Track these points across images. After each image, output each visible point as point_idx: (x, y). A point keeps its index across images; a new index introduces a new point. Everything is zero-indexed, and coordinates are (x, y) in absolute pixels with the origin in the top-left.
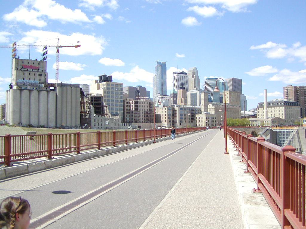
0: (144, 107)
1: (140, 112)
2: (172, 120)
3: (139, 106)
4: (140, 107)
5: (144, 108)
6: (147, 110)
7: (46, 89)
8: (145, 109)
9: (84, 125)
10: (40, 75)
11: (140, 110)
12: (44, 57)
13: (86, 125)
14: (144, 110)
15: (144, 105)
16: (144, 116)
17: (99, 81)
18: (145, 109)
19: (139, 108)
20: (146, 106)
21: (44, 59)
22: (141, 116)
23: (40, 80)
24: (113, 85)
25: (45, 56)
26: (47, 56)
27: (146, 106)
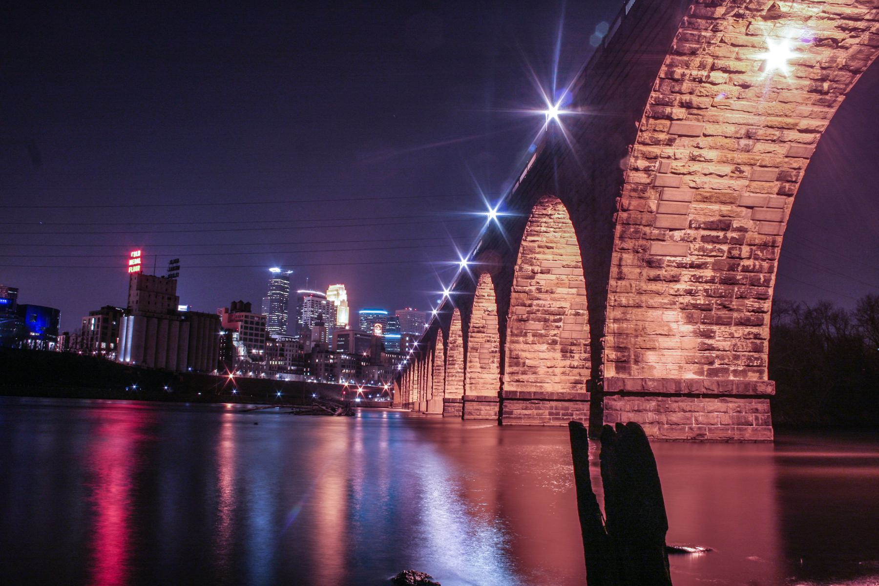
3: (285, 350)
5: (291, 353)
6: (296, 356)
7: (178, 318)
8: (293, 355)
10: (169, 299)
11: (286, 355)
12: (172, 272)
14: (291, 356)
17: (231, 310)
19: (285, 353)
21: (171, 276)
23: (169, 305)
24: (253, 317)
25: (175, 272)
26: (178, 273)
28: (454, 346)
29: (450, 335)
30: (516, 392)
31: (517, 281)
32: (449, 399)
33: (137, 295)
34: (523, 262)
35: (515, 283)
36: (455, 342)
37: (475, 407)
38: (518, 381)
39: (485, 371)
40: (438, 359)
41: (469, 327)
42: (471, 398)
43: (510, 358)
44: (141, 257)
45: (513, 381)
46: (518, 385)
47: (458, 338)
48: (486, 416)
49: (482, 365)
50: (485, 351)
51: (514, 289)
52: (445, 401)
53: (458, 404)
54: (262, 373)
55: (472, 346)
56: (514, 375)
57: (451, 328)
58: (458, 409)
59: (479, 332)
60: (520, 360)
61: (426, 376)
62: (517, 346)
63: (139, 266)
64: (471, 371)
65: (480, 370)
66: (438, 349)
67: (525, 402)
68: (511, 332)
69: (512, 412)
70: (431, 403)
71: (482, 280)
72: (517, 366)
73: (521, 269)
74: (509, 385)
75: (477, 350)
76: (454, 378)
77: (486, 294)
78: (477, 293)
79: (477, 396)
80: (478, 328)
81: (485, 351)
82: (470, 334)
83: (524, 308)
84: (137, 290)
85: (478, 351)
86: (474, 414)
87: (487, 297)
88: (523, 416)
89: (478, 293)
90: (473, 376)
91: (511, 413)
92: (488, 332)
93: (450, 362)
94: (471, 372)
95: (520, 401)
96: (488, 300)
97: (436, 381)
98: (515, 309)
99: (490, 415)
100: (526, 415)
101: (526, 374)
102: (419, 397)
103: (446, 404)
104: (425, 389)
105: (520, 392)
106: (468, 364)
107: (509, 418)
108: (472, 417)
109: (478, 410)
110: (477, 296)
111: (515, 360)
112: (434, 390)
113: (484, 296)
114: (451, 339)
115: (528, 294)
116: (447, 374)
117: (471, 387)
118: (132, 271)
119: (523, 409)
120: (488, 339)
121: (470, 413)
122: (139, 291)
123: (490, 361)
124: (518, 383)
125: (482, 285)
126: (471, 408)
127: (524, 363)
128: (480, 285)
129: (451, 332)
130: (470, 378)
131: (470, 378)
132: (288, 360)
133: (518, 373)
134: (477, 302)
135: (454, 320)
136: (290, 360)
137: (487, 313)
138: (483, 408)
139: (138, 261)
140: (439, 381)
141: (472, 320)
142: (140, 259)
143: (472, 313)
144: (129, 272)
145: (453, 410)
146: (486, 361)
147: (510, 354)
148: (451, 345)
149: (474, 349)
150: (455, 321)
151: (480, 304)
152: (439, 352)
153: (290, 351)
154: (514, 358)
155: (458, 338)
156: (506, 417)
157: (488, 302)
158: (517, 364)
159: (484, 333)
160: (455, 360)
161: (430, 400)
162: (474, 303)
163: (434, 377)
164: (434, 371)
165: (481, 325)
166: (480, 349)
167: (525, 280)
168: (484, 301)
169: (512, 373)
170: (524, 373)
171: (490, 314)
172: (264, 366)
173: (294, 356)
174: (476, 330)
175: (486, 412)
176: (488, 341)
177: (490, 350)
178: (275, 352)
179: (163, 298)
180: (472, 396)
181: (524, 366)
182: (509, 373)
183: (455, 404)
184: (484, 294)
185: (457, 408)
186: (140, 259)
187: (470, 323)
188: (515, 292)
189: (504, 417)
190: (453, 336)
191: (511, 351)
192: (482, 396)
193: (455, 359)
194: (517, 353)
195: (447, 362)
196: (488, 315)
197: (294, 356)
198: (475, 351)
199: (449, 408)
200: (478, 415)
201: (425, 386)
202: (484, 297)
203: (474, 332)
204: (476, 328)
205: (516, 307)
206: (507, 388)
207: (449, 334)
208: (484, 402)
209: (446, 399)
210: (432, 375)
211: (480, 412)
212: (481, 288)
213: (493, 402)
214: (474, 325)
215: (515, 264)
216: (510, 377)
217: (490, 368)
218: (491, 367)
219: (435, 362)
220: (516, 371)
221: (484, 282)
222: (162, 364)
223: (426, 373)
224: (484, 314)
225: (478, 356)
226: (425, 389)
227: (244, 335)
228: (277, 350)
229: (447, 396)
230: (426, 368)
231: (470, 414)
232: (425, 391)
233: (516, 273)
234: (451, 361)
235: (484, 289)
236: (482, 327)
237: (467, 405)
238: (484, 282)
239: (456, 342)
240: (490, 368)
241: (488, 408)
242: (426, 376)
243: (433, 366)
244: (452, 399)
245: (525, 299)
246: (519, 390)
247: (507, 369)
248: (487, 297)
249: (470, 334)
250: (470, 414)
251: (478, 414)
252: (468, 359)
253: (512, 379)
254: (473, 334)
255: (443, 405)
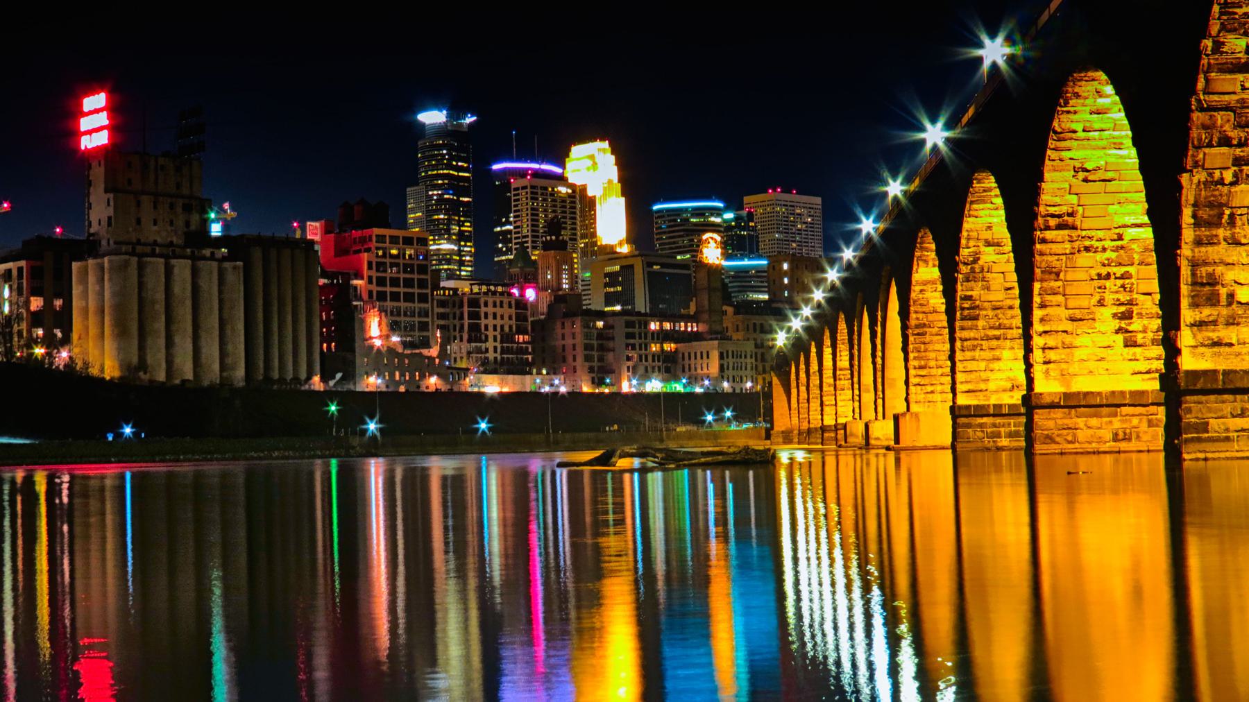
0: (498, 317)
1: (487, 337)
2: (596, 364)
4: (486, 317)
6: (510, 327)
8: (502, 327)
9: (334, 378)
13: (339, 376)
14: (499, 329)
15: (498, 310)
16: (499, 350)
18: (502, 327)
19: (483, 322)
20: (506, 317)
22: (491, 350)
23: (188, 224)
27: (506, 317)
28: (973, 270)
29: (963, 242)
30: (1215, 372)
31: (1207, 80)
32: (968, 407)
33: (109, 205)
34: (1223, 28)
35: (1201, 85)
36: (976, 260)
37: (1059, 422)
38: (1217, 344)
39: (1082, 327)
40: (919, 309)
41: (1035, 216)
42: (1047, 400)
43: (1194, 284)
44: (111, 108)
45: (1203, 345)
46: (1215, 354)
47: (983, 249)
48: (1090, 443)
49: (1071, 311)
50: (1081, 275)
51: (1199, 101)
52: (956, 412)
53: (991, 418)
54: (431, 375)
55: (1044, 265)
56: (1204, 328)
57: (966, 226)
58: (992, 432)
59: (1060, 227)
60: (1219, 287)
61: (879, 354)
62: (1212, 252)
63: (105, 133)
64: (1047, 328)
65: (1069, 326)
66: (918, 283)
67: (1239, 397)
68: (1194, 216)
69: (1207, 423)
70: (905, 424)
71: (1070, 89)
72: (1213, 305)
73: (1218, 45)
74: (1194, 355)
75: (1058, 274)
76: (977, 353)
77: (1078, 127)
78: (1056, 124)
79: (1065, 394)
80: (1059, 216)
81: (1081, 275)
82: (1038, 233)
83: (1224, 149)
84: (106, 191)
85: (1062, 276)
86: (1058, 439)
87: (1081, 134)
88: (1236, 434)
89: (1059, 125)
90: (1051, 343)
91: (1205, 427)
92: (1085, 226)
93: (966, 312)
94: (1046, 332)
95: (1226, 396)
96: (1085, 142)
97: (916, 363)
98: (1201, 156)
99: (1100, 440)
100: (1243, 430)
101: (1238, 324)
102: (857, 410)
103: (962, 420)
104: (880, 387)
105: (1226, 373)
106: (1037, 313)
107: (1199, 440)
108: (1054, 448)
109: (1070, 428)
110: (1056, 132)
111: (1208, 288)
112: (912, 389)
113: (1075, 132)
114: (964, 252)
115: (1234, 112)
116: (958, 344)
117: (1047, 372)
118: (89, 147)
119: (1234, 417)
120: (1087, 243)
121: (1048, 437)
122: (111, 196)
123: (1094, 300)
124: (1216, 349)
125: (1072, 102)
126: (1051, 424)
127: (1231, 296)
128: (1066, 104)
129: (964, 234)
130: (1044, 349)
131: (1044, 349)
132: (491, 339)
133: (1215, 323)
134: (1056, 149)
135: (972, 202)
136: (495, 340)
137: (1081, 175)
138: (1081, 422)
139: (102, 119)
140: (923, 363)
141: (1045, 198)
142: (105, 113)
143: (1042, 179)
144: (83, 148)
145: (980, 434)
146: (1084, 302)
147: (1194, 274)
148: (964, 269)
149: (1051, 273)
150: (975, 206)
151: (1066, 154)
152: (921, 291)
153: (495, 317)
154: (1203, 285)
155: (983, 249)
156: (1192, 440)
157: (1084, 148)
158: (1213, 300)
159: (1074, 228)
160: (978, 306)
161: (904, 414)
162: (1049, 152)
163: (911, 356)
164: (911, 339)
165: (1064, 209)
166: (1066, 271)
167: (1229, 76)
168: (1075, 143)
169: (1199, 325)
170: (1232, 322)
171: (1090, 178)
172: (434, 358)
173: (507, 329)
174: (1053, 222)
175: (1090, 432)
176: (1087, 249)
177: (1093, 273)
178: (457, 322)
179: (172, 206)
180: (1050, 394)
181: (1230, 304)
182: (1193, 325)
183: (985, 420)
184: (1074, 126)
185: (989, 430)
186: (105, 113)
187: (1038, 205)
188: (1202, 109)
189: (1187, 441)
190: (972, 243)
191: (1194, 265)
192: (1079, 393)
193: (977, 303)
194: (1210, 269)
195: (958, 314)
196: (1086, 180)
197: (507, 329)
198: (1053, 276)
199: (970, 430)
200: (1070, 442)
201: (879, 380)
202: (1073, 135)
203: (1048, 228)
204: (1053, 216)
205: (1207, 150)
206: (1188, 362)
207: (960, 238)
208: (1084, 406)
209: (961, 407)
210: (905, 350)
211: (1075, 436)
212: (1068, 112)
213: (1108, 406)
214: (1049, 208)
215: (1205, 33)
216: (1195, 336)
217: (1094, 319)
218: (1097, 316)
219: (913, 316)
220: (1211, 319)
221: (1077, 96)
222: (186, 370)
223: (879, 347)
224: (1074, 180)
225: (1061, 289)
226: (880, 387)
227: (378, 285)
228: (462, 318)
229: (962, 400)
230: (879, 335)
231: (1050, 439)
232: (880, 394)
233: (1205, 61)
234: (968, 309)
235: (1075, 112)
236: (1071, 215)
237: (1040, 417)
238: (1077, 96)
239: (979, 259)
240: (1094, 319)
241: (1094, 422)
242: (879, 354)
243: (905, 327)
244: (977, 407)
245: (1227, 127)
246: (1221, 366)
247: (1187, 314)
248: (1081, 134)
249: (1038, 233)
250: (1050, 439)
251: (1070, 438)
252: (1037, 299)
253: (1200, 337)
254: (1049, 235)
255: (951, 422)
